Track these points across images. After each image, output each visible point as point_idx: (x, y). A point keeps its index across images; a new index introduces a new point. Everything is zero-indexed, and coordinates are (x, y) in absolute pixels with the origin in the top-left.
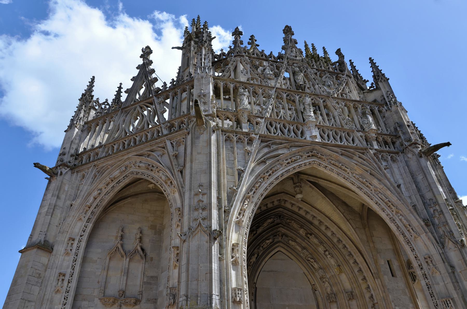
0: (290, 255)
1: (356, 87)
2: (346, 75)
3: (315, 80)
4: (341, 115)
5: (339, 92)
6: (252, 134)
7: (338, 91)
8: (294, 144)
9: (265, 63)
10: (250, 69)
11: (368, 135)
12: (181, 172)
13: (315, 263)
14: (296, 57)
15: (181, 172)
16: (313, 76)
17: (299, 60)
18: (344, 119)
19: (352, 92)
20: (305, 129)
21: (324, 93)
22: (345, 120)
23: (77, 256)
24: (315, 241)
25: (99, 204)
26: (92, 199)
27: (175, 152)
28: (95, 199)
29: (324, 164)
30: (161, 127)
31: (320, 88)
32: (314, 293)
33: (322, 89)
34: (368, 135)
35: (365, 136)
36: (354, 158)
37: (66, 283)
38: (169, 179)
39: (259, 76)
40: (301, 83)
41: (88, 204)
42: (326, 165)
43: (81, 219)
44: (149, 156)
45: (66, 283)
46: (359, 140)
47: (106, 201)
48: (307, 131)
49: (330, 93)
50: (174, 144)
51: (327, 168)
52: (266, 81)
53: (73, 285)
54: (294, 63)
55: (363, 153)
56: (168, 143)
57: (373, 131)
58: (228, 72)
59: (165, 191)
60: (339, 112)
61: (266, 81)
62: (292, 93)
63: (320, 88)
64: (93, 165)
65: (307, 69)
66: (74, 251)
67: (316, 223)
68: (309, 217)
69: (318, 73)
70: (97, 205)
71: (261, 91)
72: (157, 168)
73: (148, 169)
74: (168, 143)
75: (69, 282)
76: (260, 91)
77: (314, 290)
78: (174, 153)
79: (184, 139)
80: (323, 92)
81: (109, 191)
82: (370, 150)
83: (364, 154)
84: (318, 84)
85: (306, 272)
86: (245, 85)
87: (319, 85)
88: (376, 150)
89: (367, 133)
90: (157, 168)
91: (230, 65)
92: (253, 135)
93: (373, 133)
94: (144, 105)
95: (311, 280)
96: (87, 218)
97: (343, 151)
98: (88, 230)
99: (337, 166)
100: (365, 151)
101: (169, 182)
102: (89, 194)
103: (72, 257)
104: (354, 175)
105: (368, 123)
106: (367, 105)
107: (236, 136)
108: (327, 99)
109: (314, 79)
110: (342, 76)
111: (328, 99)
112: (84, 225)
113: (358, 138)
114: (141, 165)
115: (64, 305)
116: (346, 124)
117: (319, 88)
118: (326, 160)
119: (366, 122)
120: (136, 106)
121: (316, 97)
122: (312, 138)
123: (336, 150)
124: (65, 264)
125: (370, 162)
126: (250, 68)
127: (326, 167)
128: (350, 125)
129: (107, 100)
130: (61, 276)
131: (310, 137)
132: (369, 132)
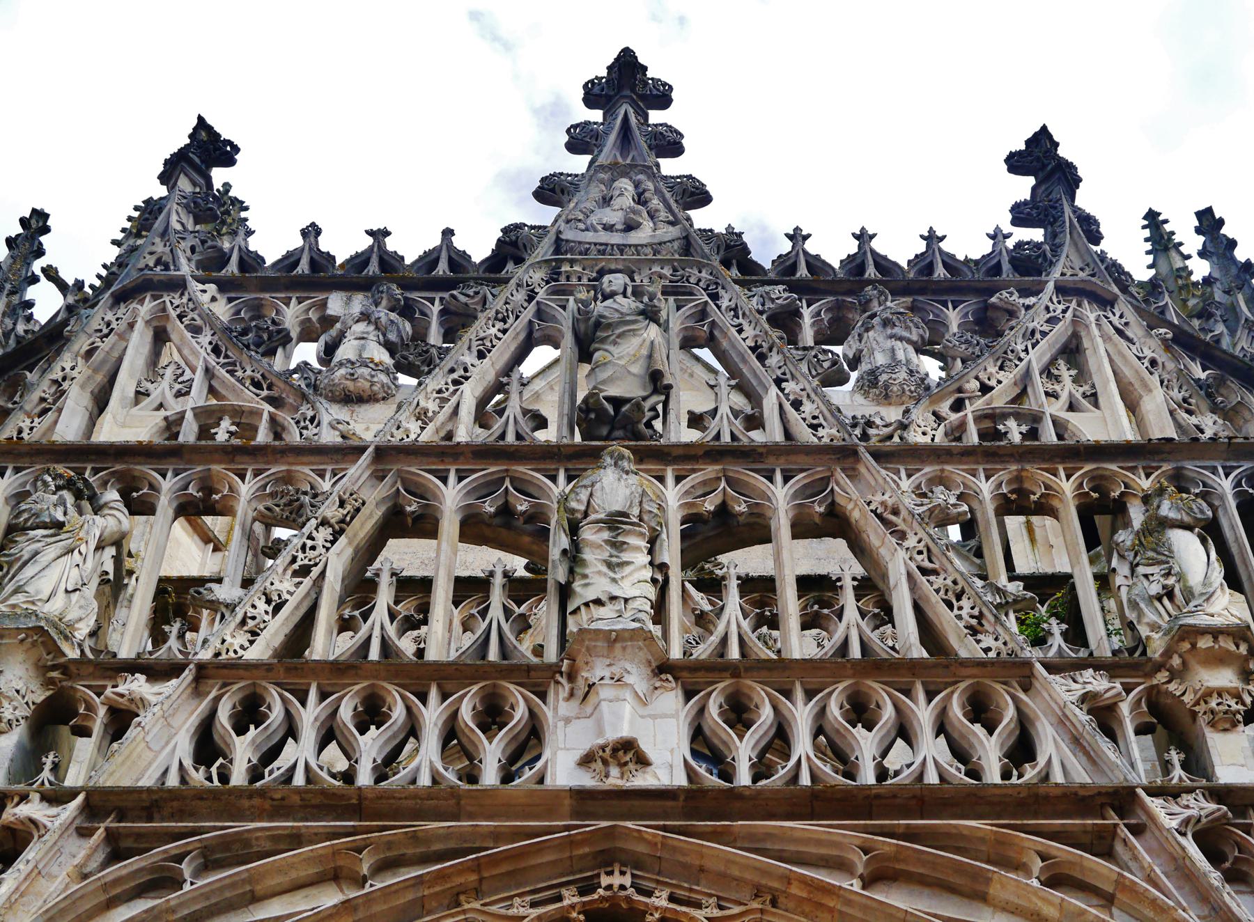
1: (1153, 363)
2: (1061, 290)
3: (762, 358)
4: (935, 572)
5: (969, 410)
6: (24, 798)
7: (958, 406)
8: (414, 838)
9: (336, 304)
10: (212, 360)
11: (1172, 687)
14: (630, 227)
16: (749, 331)
17: (656, 247)
18: (959, 598)
19: (1101, 400)
21: (821, 432)
22: (965, 602)
31: (797, 405)
33: (808, 407)
34: (1172, 687)
36: (994, 890)
39: (265, 393)
40: (613, 391)
46: (1076, 742)
48: (567, 721)
49: (870, 424)
52: (310, 414)
54: (601, 273)
55: (1103, 845)
57: (1204, 643)
58: (45, 412)
60: (921, 546)
61: (312, 420)
62: (522, 469)
63: (797, 405)
65: (715, 297)
69: (807, 313)
80: (814, 427)
82: (1155, 805)
83: (1109, 854)
84: (778, 382)
86: (118, 467)
87: (790, 386)
88: (1220, 794)
89: (1162, 677)
91: (68, 366)
93: (1218, 659)
97: (887, 844)
100: (1113, 819)
105: (1170, 594)
106: (1214, 471)
108: (840, 475)
109: (753, 349)
110: (1022, 301)
111: (853, 475)
113: (1063, 722)
116: (974, 631)
117: (787, 406)
119: (1155, 589)
121: (739, 471)
122: (598, 765)
123: (819, 842)
125: (1154, 902)
126: (216, 350)
128: (1000, 630)
131: (586, 761)
132: (1176, 661)
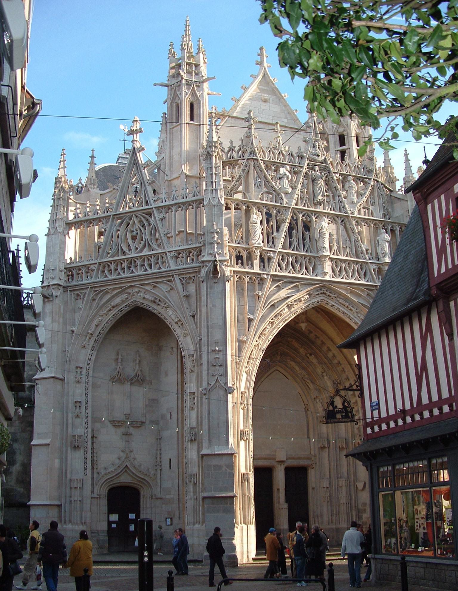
0: (287, 374)
12: (194, 316)
13: (311, 384)
15: (194, 316)
20: (318, 263)
23: (88, 384)
24: (315, 361)
25: (101, 332)
26: (93, 326)
27: (187, 293)
28: (97, 326)
29: (331, 302)
30: (166, 254)
32: (306, 412)
34: (382, 267)
35: (379, 268)
37: (83, 409)
38: (180, 321)
41: (90, 332)
42: (334, 304)
43: (85, 347)
44: (155, 287)
45: (83, 409)
47: (109, 328)
50: (184, 281)
51: (334, 307)
53: (90, 410)
56: (177, 278)
59: (175, 331)
62: (308, 212)
64: (89, 287)
66: (84, 379)
67: (319, 342)
68: (312, 336)
70: (100, 333)
71: (275, 212)
72: (165, 304)
73: (154, 302)
74: (177, 278)
75: (86, 409)
76: (274, 213)
77: (306, 410)
78: (184, 294)
79: (194, 277)
81: (111, 319)
85: (302, 393)
89: (381, 265)
90: (165, 304)
92: (265, 276)
94: (141, 215)
95: (305, 400)
96: (91, 347)
98: (93, 358)
99: (344, 305)
101: (180, 324)
102: (91, 321)
103: (84, 385)
104: (359, 315)
107: (247, 277)
112: (89, 353)
114: (146, 296)
115: (86, 429)
118: (334, 298)
120: (132, 214)
124: (78, 391)
127: (333, 305)
129: (80, 180)
130: (78, 403)
